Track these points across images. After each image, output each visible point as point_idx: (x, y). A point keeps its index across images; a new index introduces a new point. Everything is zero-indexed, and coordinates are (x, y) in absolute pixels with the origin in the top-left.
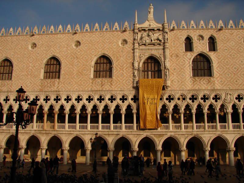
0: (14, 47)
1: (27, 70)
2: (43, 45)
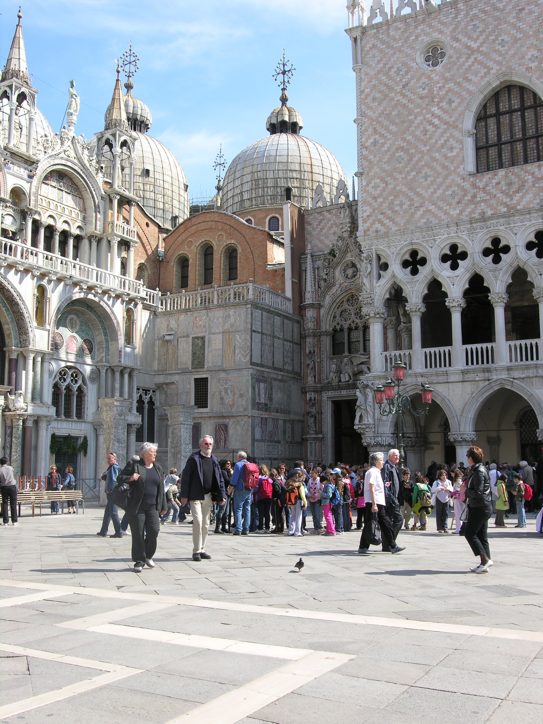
0: (531, 27)
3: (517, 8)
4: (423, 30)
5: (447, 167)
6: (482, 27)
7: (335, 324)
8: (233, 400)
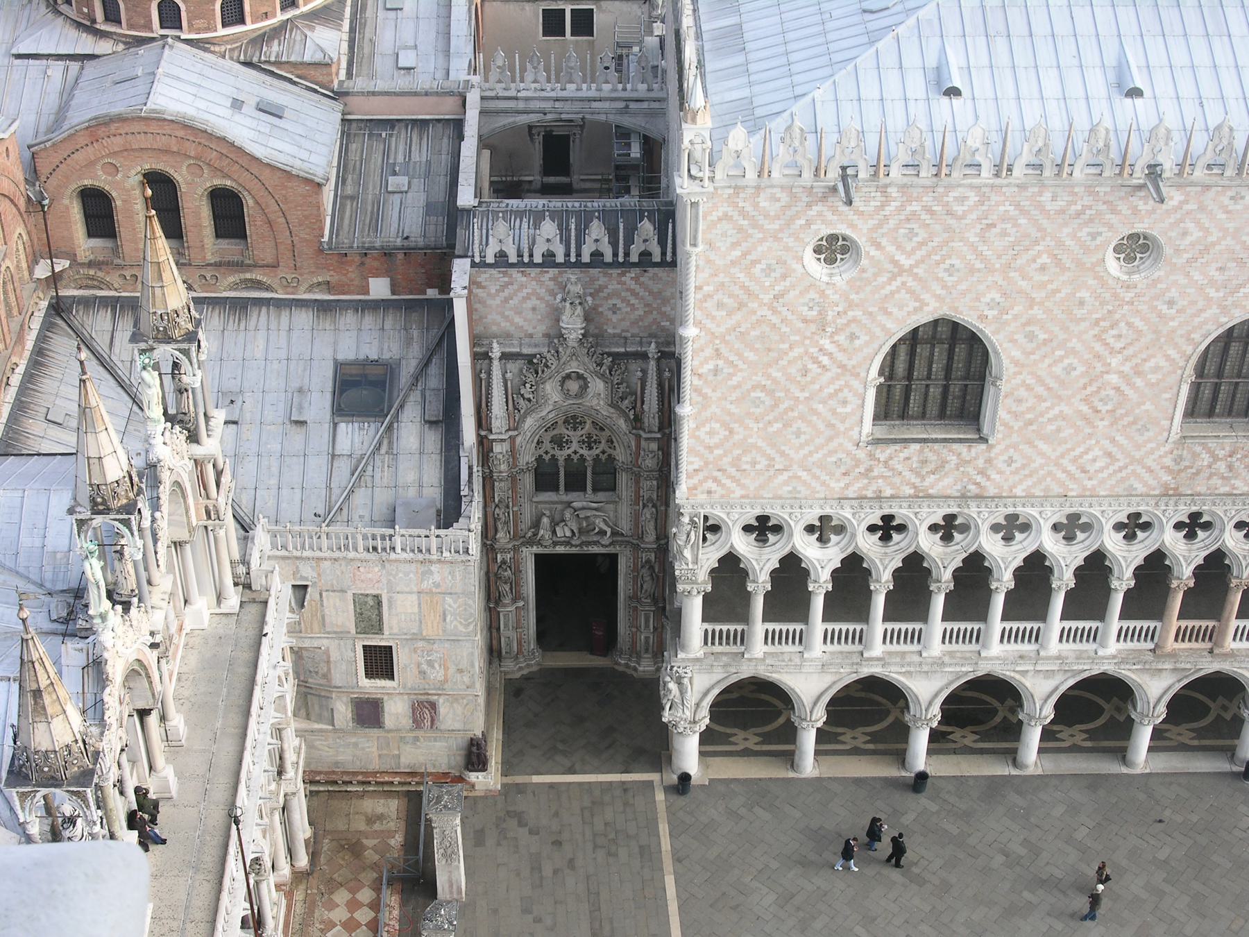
0: (999, 257)
1: (1089, 390)
2: (1207, 249)
3: (985, 222)
4: (820, 214)
5: (833, 426)
6: (922, 235)
7: (541, 452)
8: (445, 675)
